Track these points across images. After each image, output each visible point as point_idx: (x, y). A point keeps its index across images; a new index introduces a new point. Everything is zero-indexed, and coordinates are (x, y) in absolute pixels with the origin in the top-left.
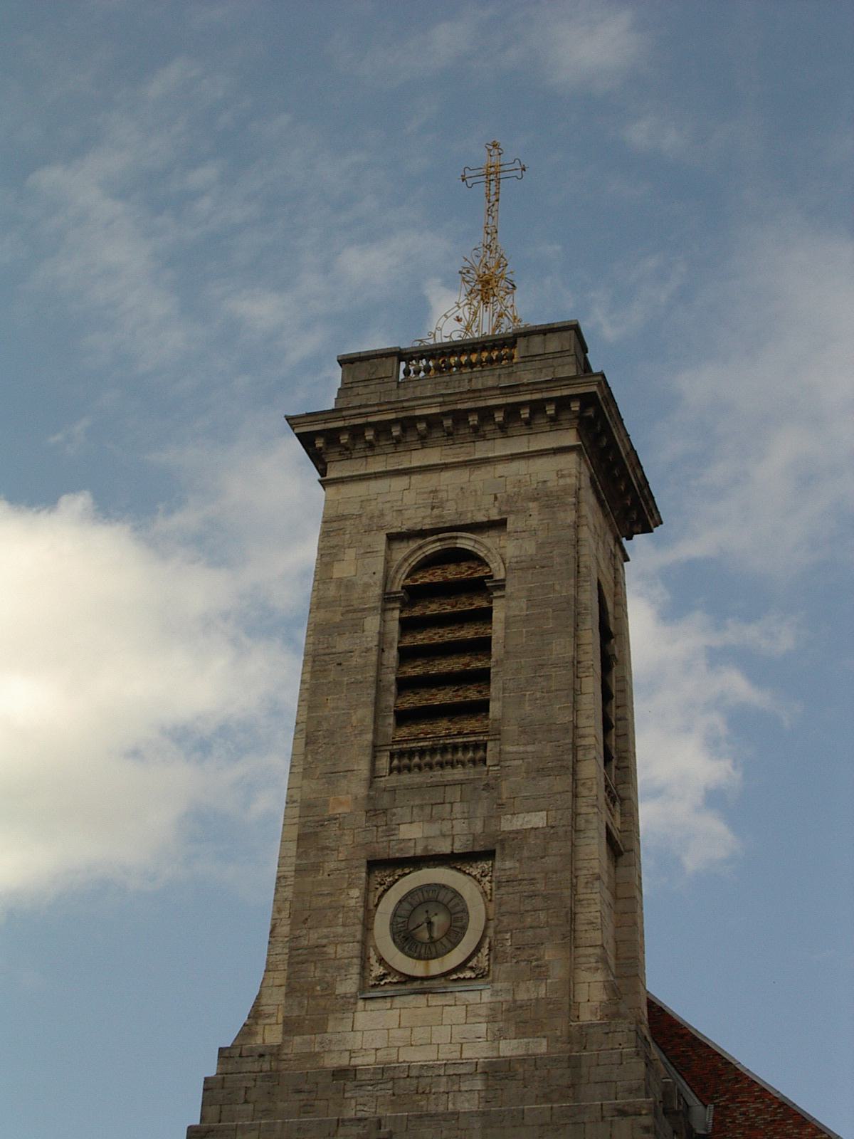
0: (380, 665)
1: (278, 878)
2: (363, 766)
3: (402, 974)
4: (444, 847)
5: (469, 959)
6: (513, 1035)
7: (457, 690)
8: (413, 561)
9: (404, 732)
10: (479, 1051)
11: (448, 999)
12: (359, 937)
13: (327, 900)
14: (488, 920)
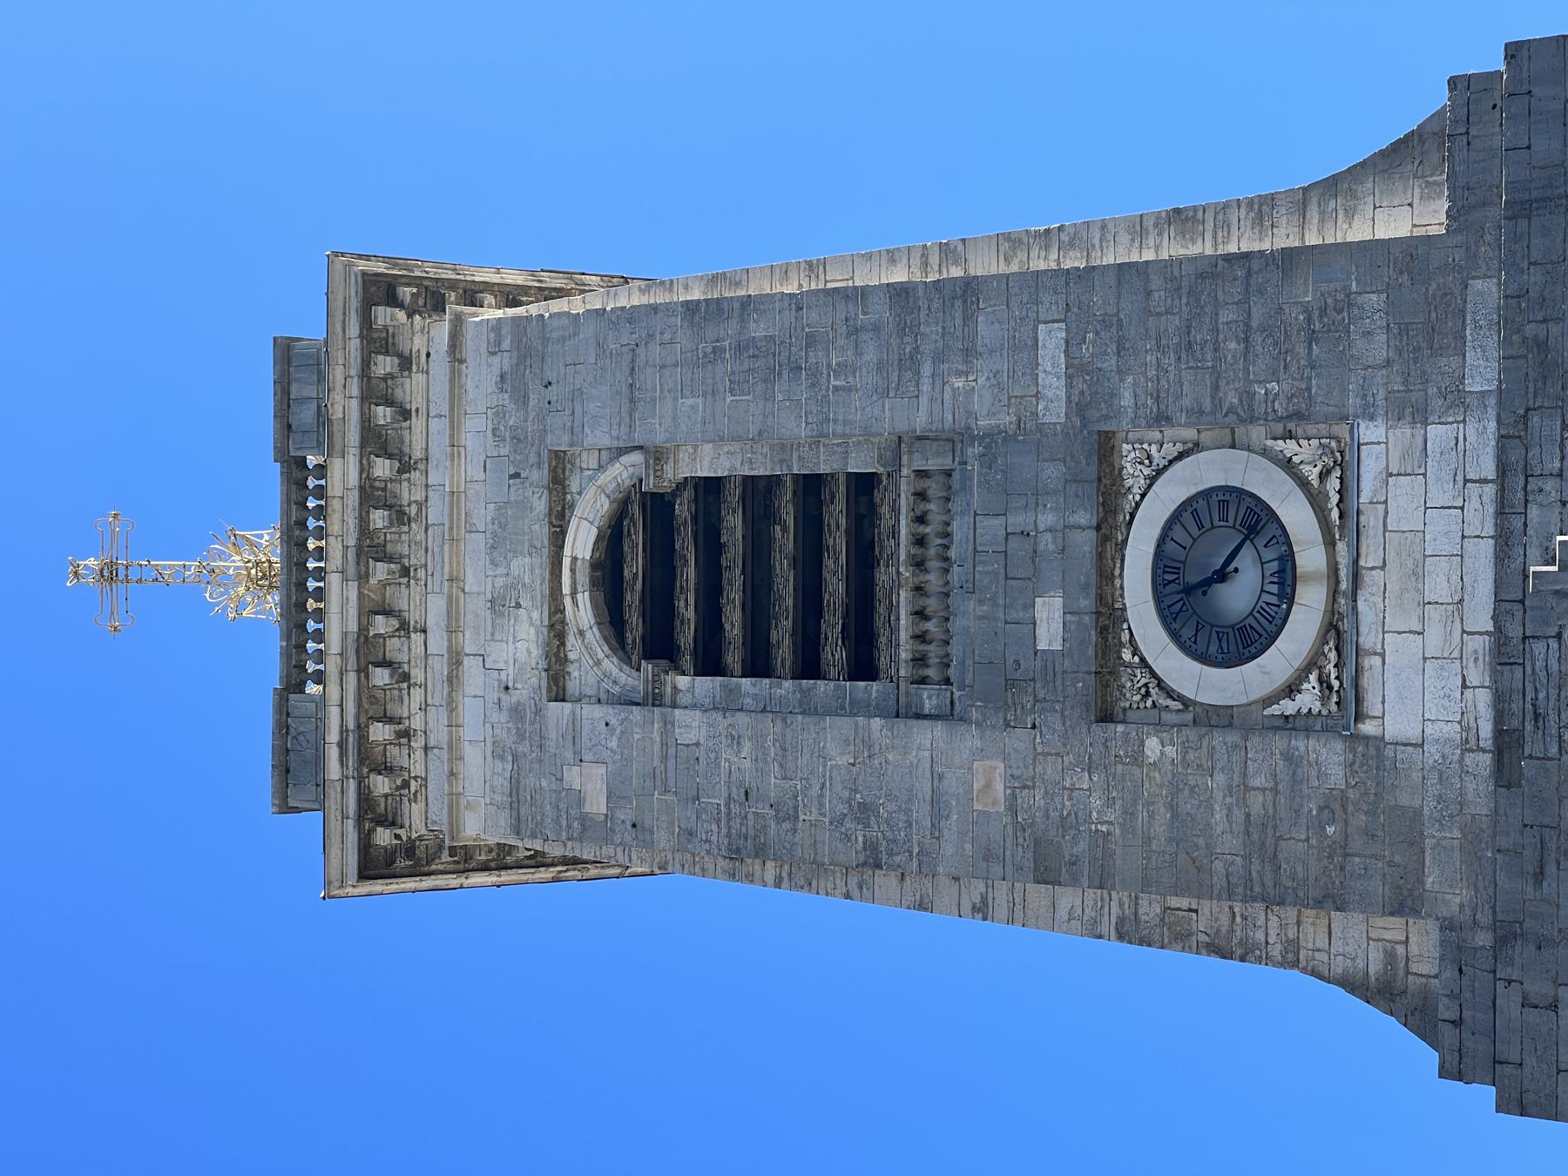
2: (926, 736)
4: (1085, 541)
5: (1303, 483)
8: (601, 650)
10: (1479, 440)
11: (1371, 520)
12: (1233, 737)
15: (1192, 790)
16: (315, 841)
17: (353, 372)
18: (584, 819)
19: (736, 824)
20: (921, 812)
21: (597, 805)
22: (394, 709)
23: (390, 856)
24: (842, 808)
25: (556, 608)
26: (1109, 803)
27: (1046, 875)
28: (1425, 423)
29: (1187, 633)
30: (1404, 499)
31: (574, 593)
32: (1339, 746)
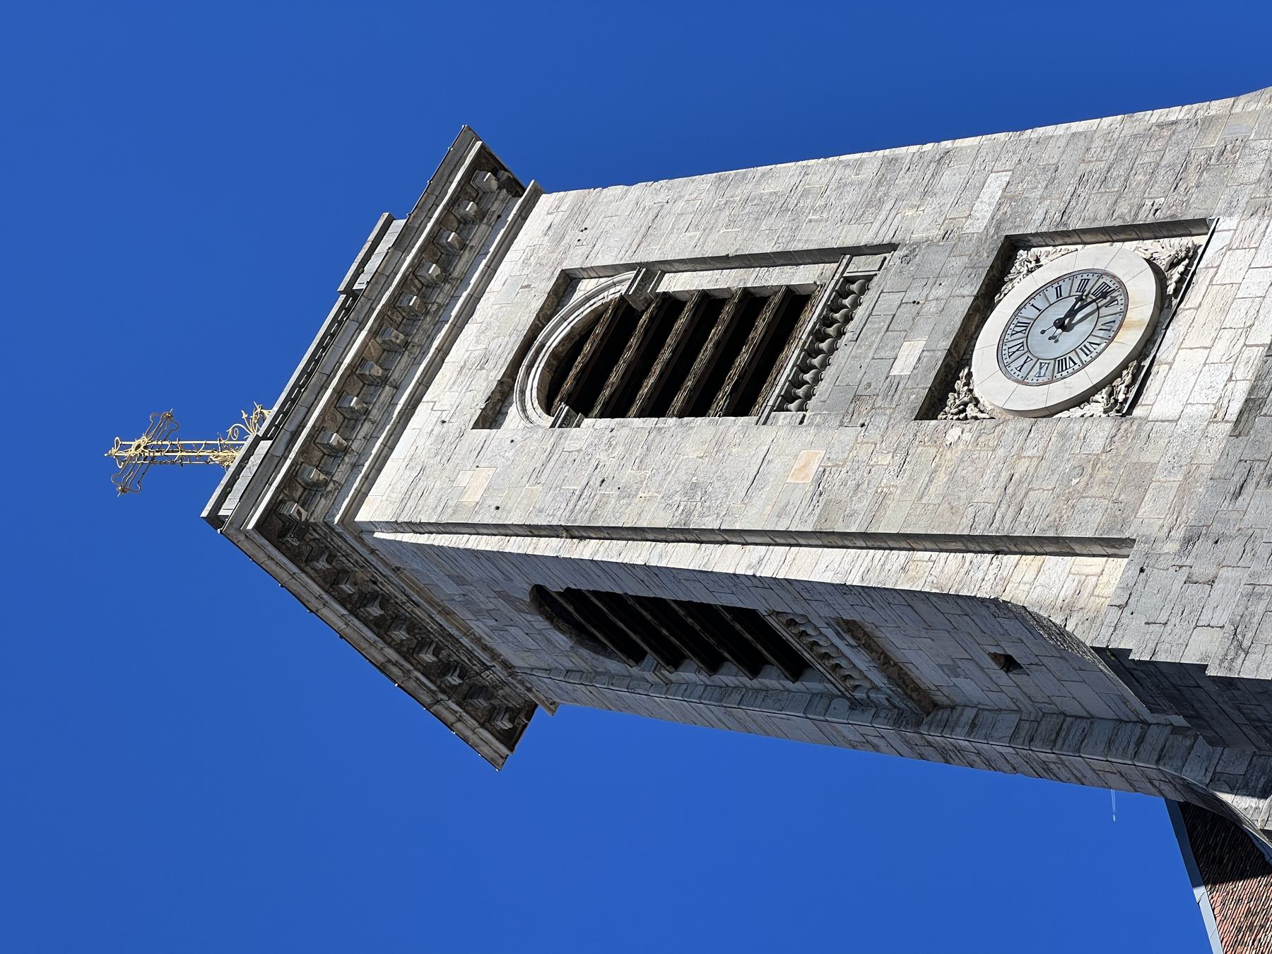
3: (1124, 366)
13: (942, 478)
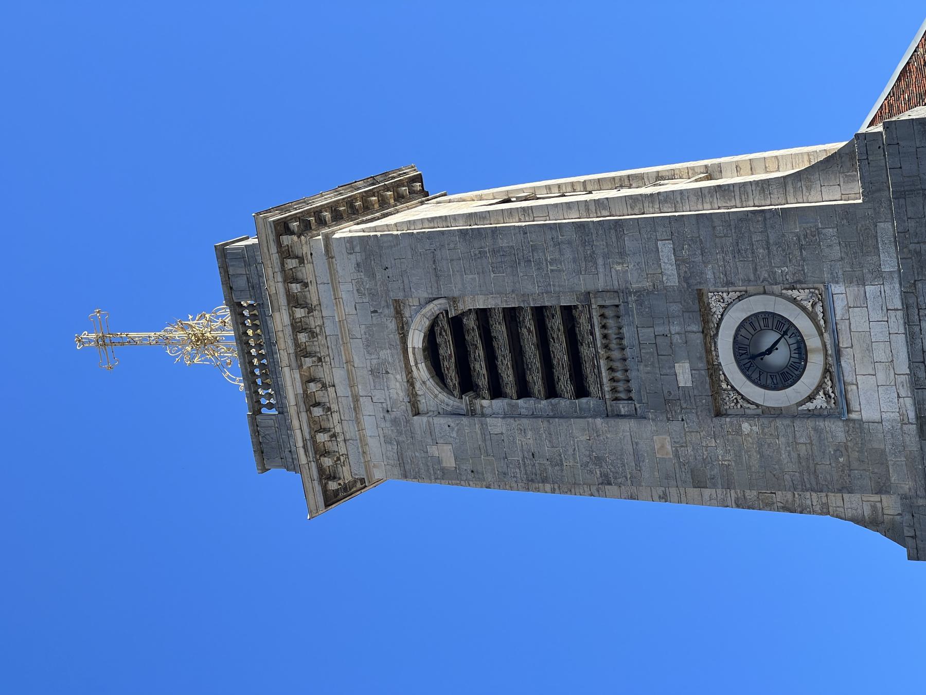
0: (533, 416)
1: (738, 506)
2: (626, 426)
4: (697, 339)
5: (804, 309)
6: (875, 258)
7: (553, 338)
8: (436, 390)
9: (593, 389)
10: (893, 294)
11: (843, 327)
12: (787, 422)
14: (765, 293)
15: (769, 445)
16: (291, 487)
17: (277, 270)
18: (443, 470)
19: (529, 468)
20: (629, 460)
21: (449, 462)
22: (325, 424)
23: (336, 492)
24: (586, 459)
25: (409, 371)
26: (727, 452)
27: (699, 484)
28: (864, 285)
29: (755, 376)
30: (858, 319)
31: (416, 364)
32: (841, 424)
